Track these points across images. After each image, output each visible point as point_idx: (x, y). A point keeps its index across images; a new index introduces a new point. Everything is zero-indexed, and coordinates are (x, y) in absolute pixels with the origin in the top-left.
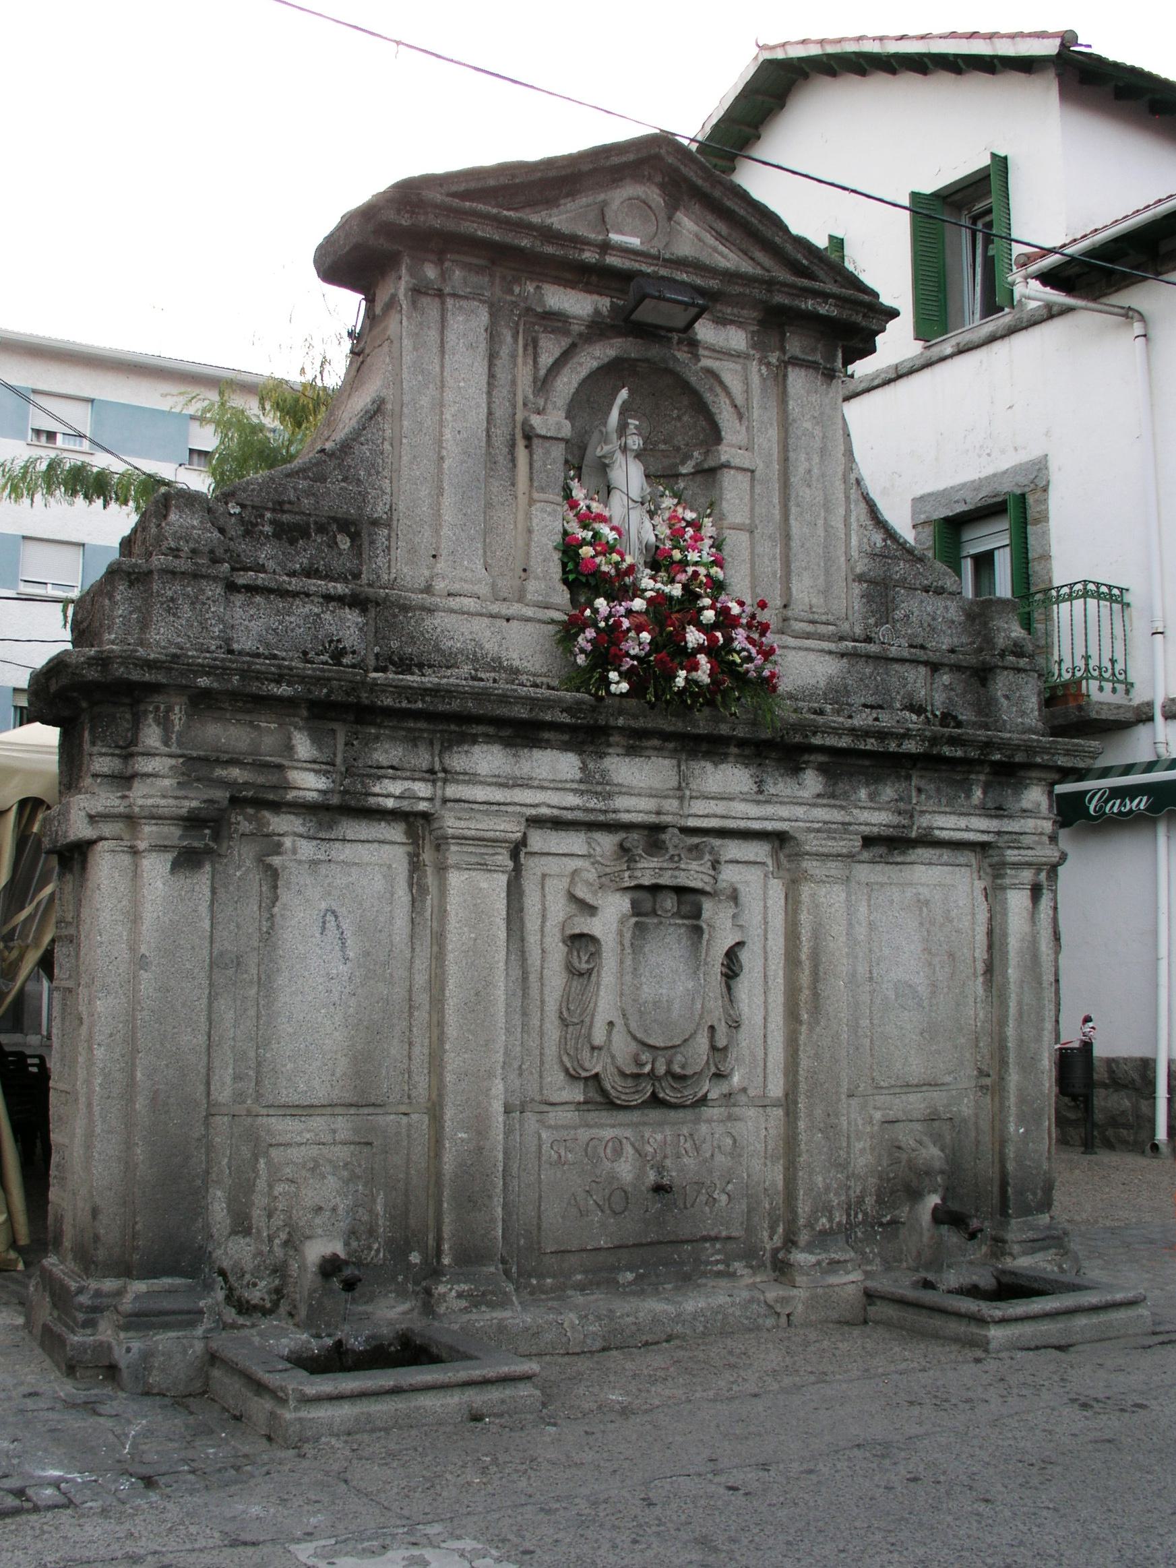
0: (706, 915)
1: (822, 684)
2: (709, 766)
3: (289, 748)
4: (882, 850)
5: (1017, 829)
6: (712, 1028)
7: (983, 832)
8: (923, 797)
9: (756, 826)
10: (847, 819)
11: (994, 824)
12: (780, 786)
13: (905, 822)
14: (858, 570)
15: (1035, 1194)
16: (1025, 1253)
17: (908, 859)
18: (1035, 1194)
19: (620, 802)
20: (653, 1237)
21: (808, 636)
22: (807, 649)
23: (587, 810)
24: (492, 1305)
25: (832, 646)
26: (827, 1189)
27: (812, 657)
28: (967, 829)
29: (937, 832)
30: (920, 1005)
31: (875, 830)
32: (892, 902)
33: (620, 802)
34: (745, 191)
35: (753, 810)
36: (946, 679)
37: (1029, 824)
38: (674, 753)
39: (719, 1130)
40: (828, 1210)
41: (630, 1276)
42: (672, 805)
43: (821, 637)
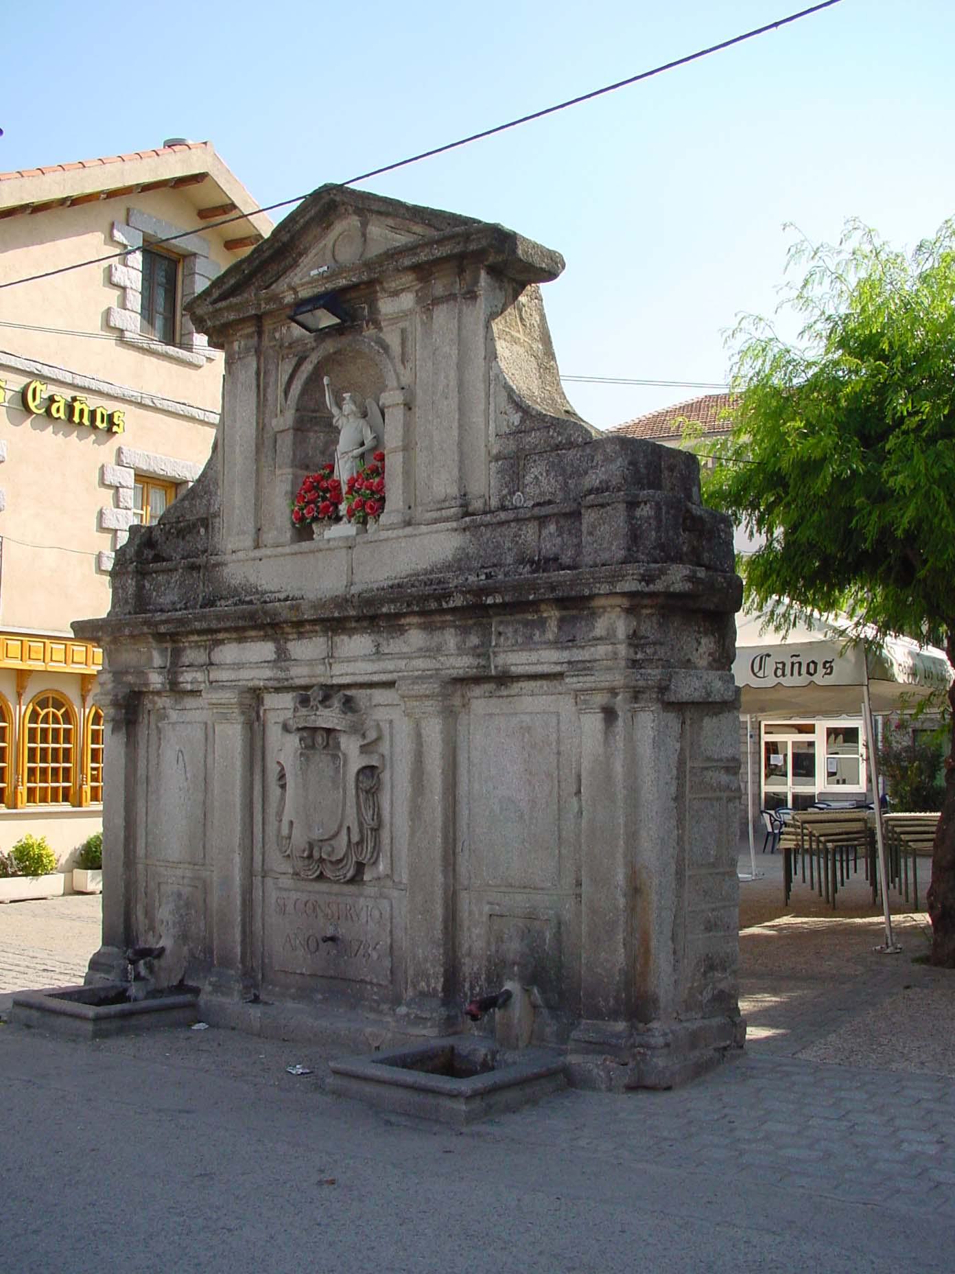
0: (343, 746)
1: (450, 558)
2: (346, 638)
3: (151, 659)
4: (492, 686)
5: (587, 657)
6: (348, 828)
7: (556, 663)
8: (502, 639)
9: (376, 678)
10: (438, 666)
11: (565, 655)
12: (395, 645)
13: (483, 663)
14: (494, 452)
15: (606, 1000)
16: (576, 1052)
17: (513, 692)
18: (606, 1000)
19: (294, 671)
20: (332, 973)
21: (435, 521)
22: (436, 532)
23: (278, 680)
24: (223, 994)
25: (454, 524)
26: (426, 960)
27: (442, 536)
28: (539, 663)
29: (513, 668)
30: (521, 817)
31: (461, 672)
32: (499, 729)
33: (294, 671)
34: (42, 243)
35: (371, 667)
36: (552, 528)
37: (602, 650)
38: (325, 631)
39: (371, 903)
40: (427, 978)
41: (320, 996)
42: (320, 669)
43: (446, 520)
